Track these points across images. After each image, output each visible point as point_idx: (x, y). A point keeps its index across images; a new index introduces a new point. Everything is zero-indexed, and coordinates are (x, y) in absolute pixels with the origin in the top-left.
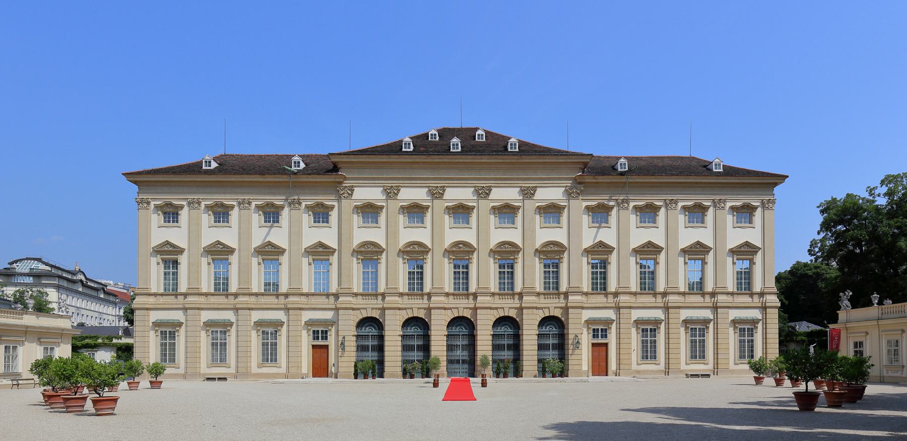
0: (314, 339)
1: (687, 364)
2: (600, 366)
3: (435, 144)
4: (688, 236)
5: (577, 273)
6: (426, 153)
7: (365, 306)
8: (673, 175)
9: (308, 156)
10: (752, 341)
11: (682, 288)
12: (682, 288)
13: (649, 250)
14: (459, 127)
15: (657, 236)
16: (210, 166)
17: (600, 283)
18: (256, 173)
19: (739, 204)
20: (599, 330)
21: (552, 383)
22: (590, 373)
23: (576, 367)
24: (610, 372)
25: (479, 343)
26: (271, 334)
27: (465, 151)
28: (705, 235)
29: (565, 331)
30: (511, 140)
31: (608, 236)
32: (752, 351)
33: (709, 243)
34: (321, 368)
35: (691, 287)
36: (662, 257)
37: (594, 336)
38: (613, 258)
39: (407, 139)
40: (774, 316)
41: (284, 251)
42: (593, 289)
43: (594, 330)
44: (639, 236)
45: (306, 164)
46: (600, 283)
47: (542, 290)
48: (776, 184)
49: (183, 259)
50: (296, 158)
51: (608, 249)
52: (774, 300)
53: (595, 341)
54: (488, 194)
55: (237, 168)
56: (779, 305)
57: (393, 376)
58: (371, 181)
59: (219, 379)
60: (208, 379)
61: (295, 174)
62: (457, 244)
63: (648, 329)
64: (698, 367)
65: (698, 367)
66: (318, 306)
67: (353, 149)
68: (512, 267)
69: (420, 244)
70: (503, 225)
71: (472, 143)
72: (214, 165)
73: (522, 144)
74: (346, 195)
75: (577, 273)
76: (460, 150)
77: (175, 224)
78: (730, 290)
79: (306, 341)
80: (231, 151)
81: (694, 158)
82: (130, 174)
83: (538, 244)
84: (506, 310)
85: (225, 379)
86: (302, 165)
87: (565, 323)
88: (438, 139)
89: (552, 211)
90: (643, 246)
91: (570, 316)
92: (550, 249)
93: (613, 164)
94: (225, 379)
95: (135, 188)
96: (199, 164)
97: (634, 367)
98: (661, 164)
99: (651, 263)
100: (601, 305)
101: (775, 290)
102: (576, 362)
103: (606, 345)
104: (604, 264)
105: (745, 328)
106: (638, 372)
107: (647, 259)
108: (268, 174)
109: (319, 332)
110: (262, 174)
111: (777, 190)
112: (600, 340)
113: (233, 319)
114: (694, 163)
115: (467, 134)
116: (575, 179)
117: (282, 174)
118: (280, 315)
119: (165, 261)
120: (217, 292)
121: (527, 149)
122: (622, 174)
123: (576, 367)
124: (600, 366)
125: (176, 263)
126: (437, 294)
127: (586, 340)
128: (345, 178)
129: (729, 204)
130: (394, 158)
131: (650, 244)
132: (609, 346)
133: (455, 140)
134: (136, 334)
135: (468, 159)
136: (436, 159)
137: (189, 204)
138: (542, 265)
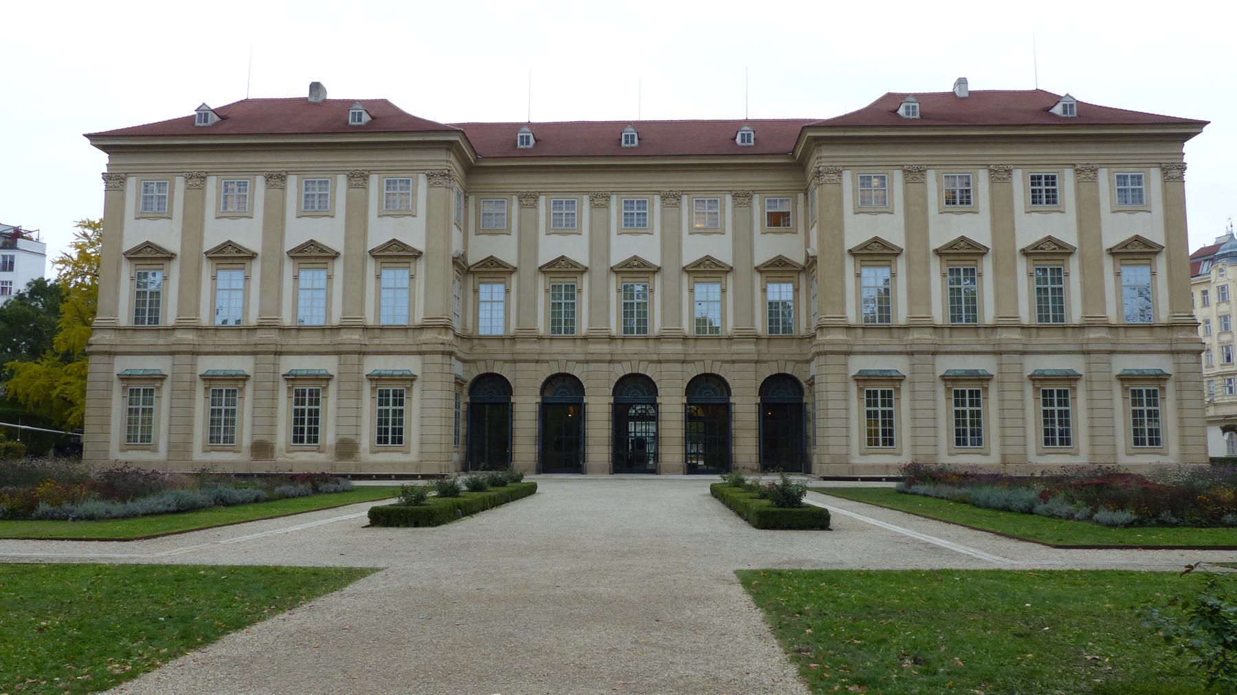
26: (311, 394)
33: (1071, 239)
48: (1189, 136)
95: (103, 157)
111: (1190, 147)
118: (327, 364)
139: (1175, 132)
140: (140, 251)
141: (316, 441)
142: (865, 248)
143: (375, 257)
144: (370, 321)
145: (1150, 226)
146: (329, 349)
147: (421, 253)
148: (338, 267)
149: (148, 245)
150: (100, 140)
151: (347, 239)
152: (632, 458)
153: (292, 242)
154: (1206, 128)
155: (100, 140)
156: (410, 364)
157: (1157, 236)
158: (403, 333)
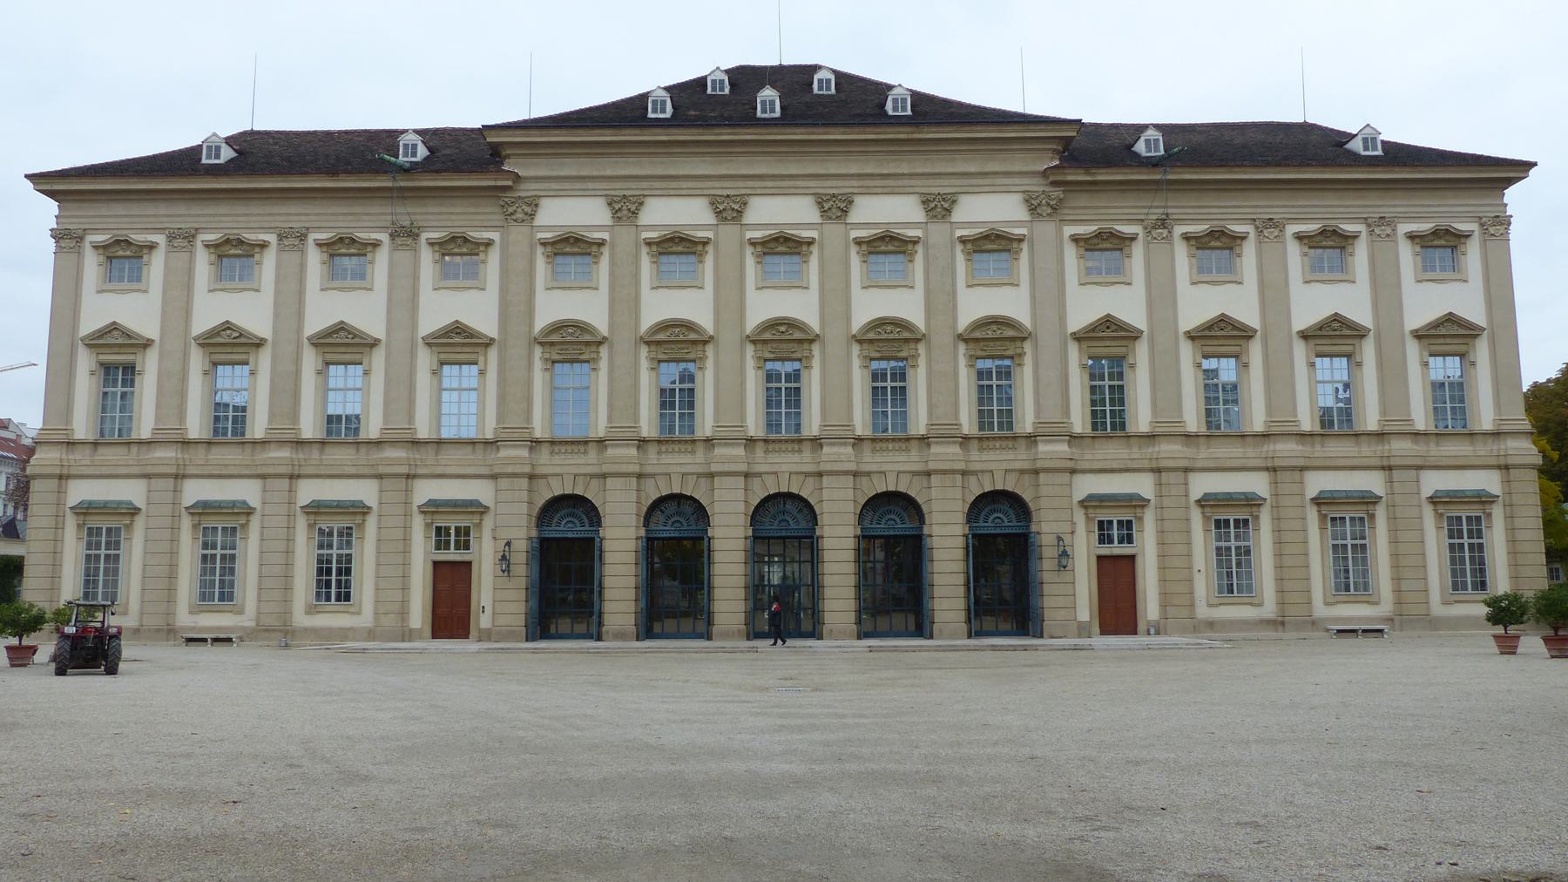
0: (438, 548)
1: (1327, 604)
2: (1118, 609)
4: (1312, 303)
5: (1050, 391)
6: (704, 123)
7: (557, 470)
10: (1481, 546)
11: (1307, 423)
12: (1307, 423)
13: (1222, 335)
14: (776, 63)
15: (1239, 302)
16: (218, 156)
17: (1109, 414)
19: (1425, 227)
20: (1115, 522)
21: (1003, 651)
22: (1097, 629)
23: (1061, 615)
24: (1142, 626)
25: (827, 556)
26: (340, 534)
27: (790, 117)
28: (1351, 300)
29: (1034, 528)
30: (895, 91)
31: (1128, 304)
32: (1482, 571)
34: (451, 614)
35: (1326, 418)
36: (1255, 351)
37: (1101, 541)
38: (1141, 353)
40: (1529, 490)
41: (374, 344)
42: (1095, 426)
43: (1101, 523)
44: (1199, 305)
45: (429, 149)
46: (1109, 414)
47: (975, 431)
48: (1510, 182)
49: (150, 365)
50: (412, 138)
51: (1129, 335)
52: (1526, 450)
53: (1106, 550)
54: (845, 212)
55: (277, 160)
56: (1539, 460)
58: (578, 185)
59: (216, 640)
60: (190, 640)
61: (406, 171)
62: (773, 324)
63: (1231, 518)
64: (1354, 612)
65: (1354, 612)
66: (450, 470)
67: (535, 115)
68: (903, 377)
69: (688, 326)
71: (807, 98)
72: (227, 154)
73: (919, 99)
74: (520, 215)
75: (1050, 391)
76: (778, 114)
77: (135, 286)
78: (1420, 425)
79: (421, 554)
80: (268, 122)
81: (1314, 126)
83: (964, 322)
84: (891, 479)
85: (229, 640)
86: (422, 152)
87: (1032, 506)
88: (727, 91)
89: (992, 243)
90: (1210, 326)
91: (1044, 491)
92: (990, 335)
93: (1130, 140)
94: (229, 640)
95: (52, 206)
96: (195, 151)
97: (1203, 612)
98: (1238, 140)
99: (1227, 370)
100: (1115, 465)
101: (1526, 425)
103: (1132, 558)
104: (1119, 365)
105: (1464, 520)
106: (1211, 625)
107: (1219, 356)
109: (453, 528)
110: (333, 172)
111: (1512, 194)
112: (1117, 549)
113: (254, 502)
115: (794, 79)
116: (1045, 174)
119: (108, 369)
120: (220, 438)
121: (933, 113)
122: (1154, 163)
123: (1061, 615)
124: (1118, 609)
125: (130, 370)
126: (728, 441)
127: (1084, 549)
128: (517, 178)
129: (1404, 228)
131: (1223, 321)
132: (1139, 561)
133: (768, 93)
134: (30, 534)
136: (725, 135)
137: (171, 238)
138: (974, 376)
139: (1498, 174)
140: (101, 337)
141: (347, 597)
142: (1093, 330)
143: (429, 345)
144: (423, 433)
145: (1464, 299)
146: (366, 471)
147: (492, 340)
148: (378, 359)
149: (114, 327)
150: (45, 182)
151: (389, 322)
152: (784, 615)
153: (315, 323)
154: (1533, 172)
155: (45, 182)
156: (479, 491)
157: (1474, 313)
158: (470, 448)
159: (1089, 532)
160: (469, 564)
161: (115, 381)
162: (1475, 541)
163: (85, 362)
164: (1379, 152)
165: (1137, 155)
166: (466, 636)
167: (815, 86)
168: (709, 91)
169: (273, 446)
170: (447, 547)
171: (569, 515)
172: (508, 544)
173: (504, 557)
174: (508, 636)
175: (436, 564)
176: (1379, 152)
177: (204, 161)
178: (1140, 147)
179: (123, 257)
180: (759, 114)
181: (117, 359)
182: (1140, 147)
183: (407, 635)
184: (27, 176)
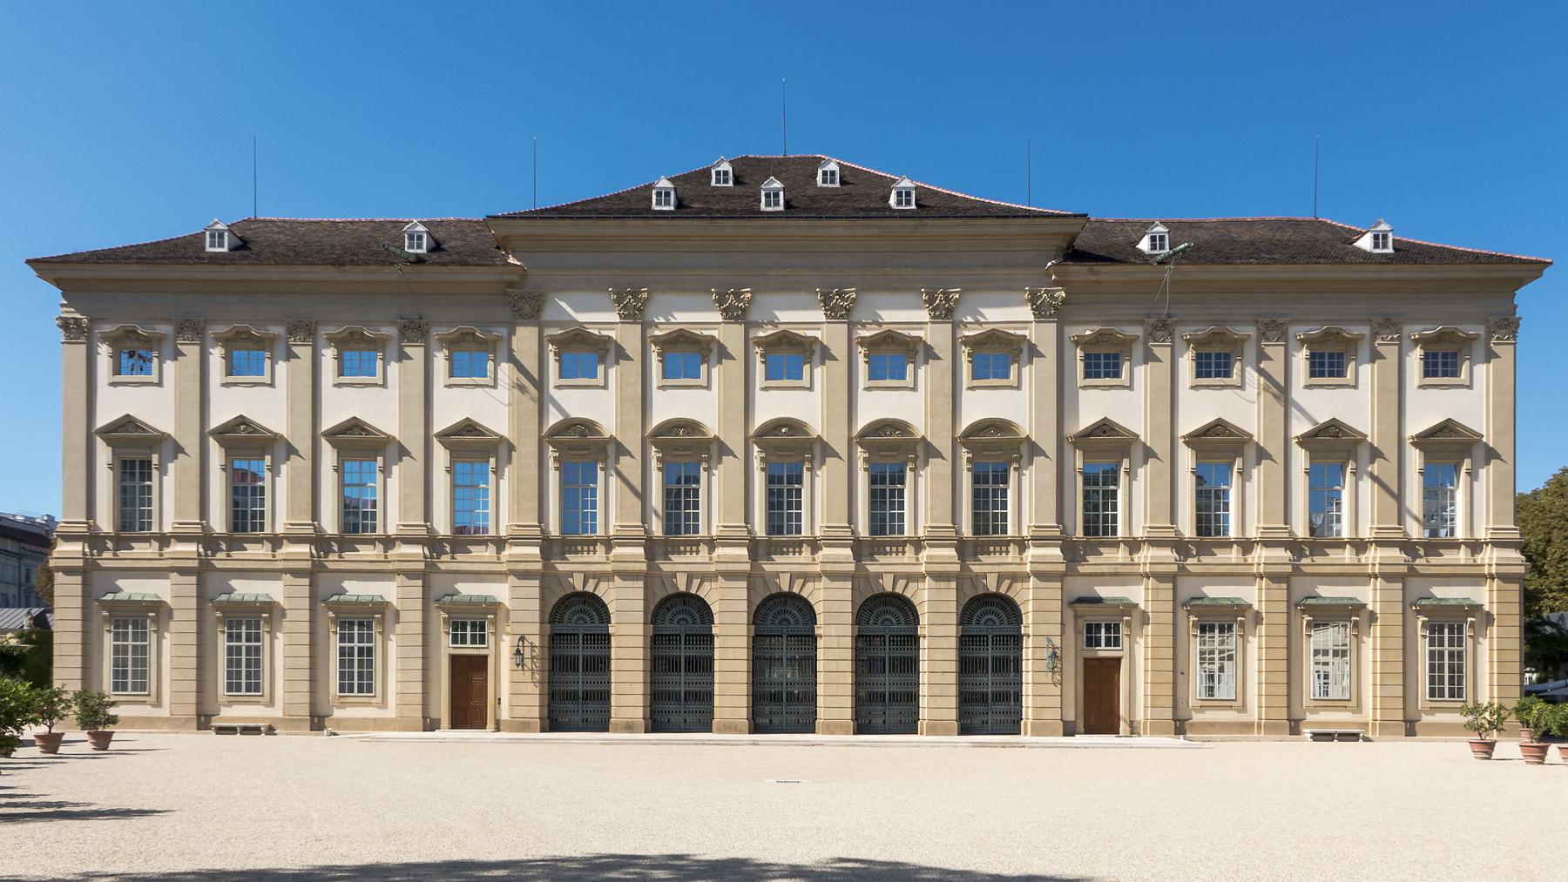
0: (455, 641)
3: (726, 194)
6: (708, 214)
8: (1276, 262)
9: (440, 223)
18: (324, 262)
39: (664, 183)
48: (1521, 282)
55: (282, 249)
57: (629, 728)
70: (882, 383)
71: (811, 192)
76: (781, 208)
82: (65, 260)
95: (56, 293)
98: (1246, 237)
102: (1048, 701)
108: (352, 263)
110: (338, 263)
111: (1523, 296)
114: (1323, 235)
115: (799, 170)
117: (383, 263)
130: (634, 227)
135: (800, 227)
136: (729, 227)
159: (1077, 632)
160: (486, 657)
161: (133, 475)
162: (1455, 648)
163: (104, 454)
164: (1390, 250)
165: (1141, 253)
166: (483, 726)
167: (819, 178)
168: (713, 183)
169: (321, 696)
170: (464, 641)
171: (581, 611)
172: (522, 639)
173: (518, 652)
174: (524, 726)
175: (454, 659)
176: (1390, 250)
177: (208, 249)
178: (1144, 245)
179: (135, 353)
180: (763, 207)
181: (137, 453)
182: (1144, 245)
183: (431, 725)
184: (28, 262)
